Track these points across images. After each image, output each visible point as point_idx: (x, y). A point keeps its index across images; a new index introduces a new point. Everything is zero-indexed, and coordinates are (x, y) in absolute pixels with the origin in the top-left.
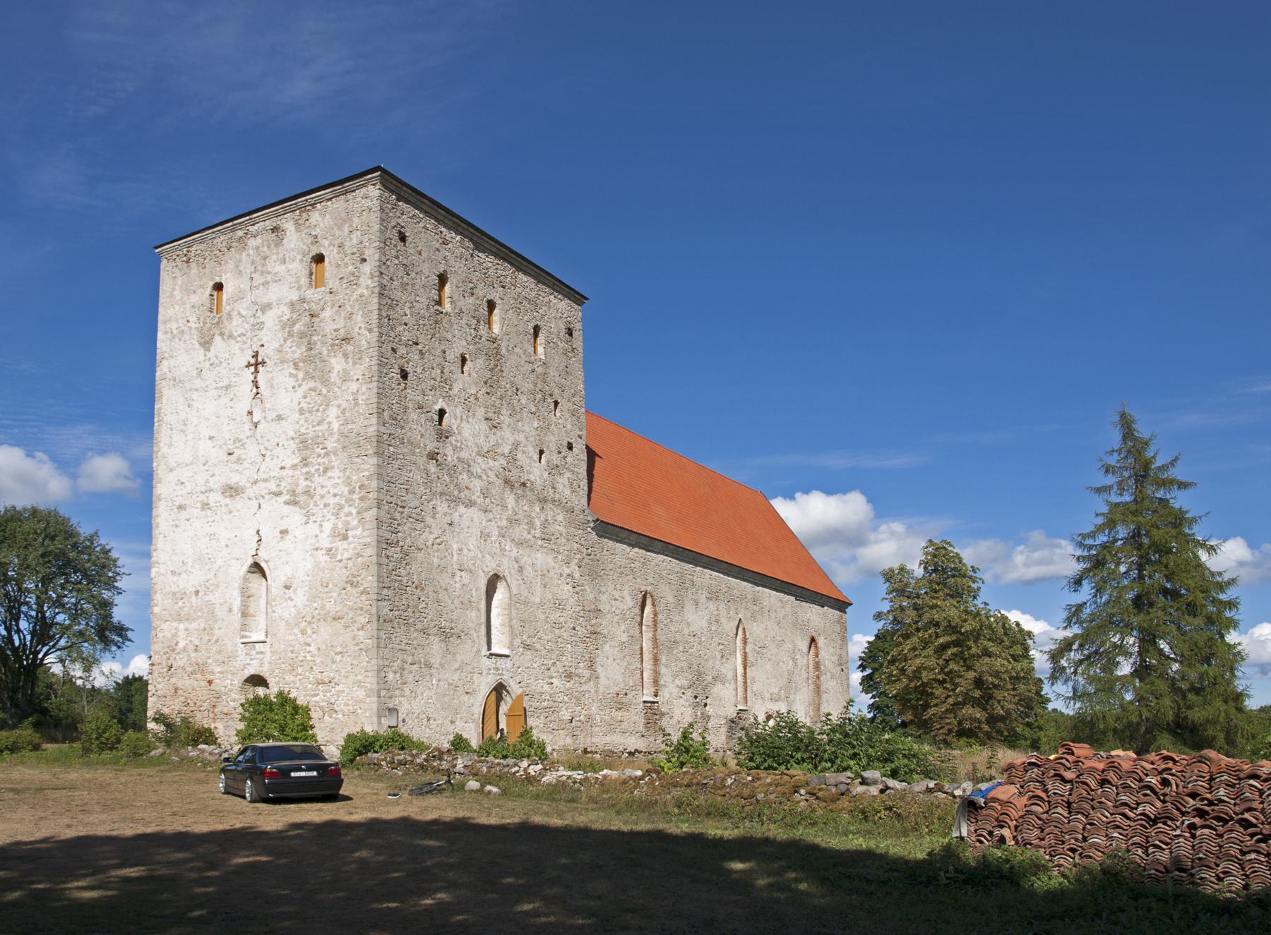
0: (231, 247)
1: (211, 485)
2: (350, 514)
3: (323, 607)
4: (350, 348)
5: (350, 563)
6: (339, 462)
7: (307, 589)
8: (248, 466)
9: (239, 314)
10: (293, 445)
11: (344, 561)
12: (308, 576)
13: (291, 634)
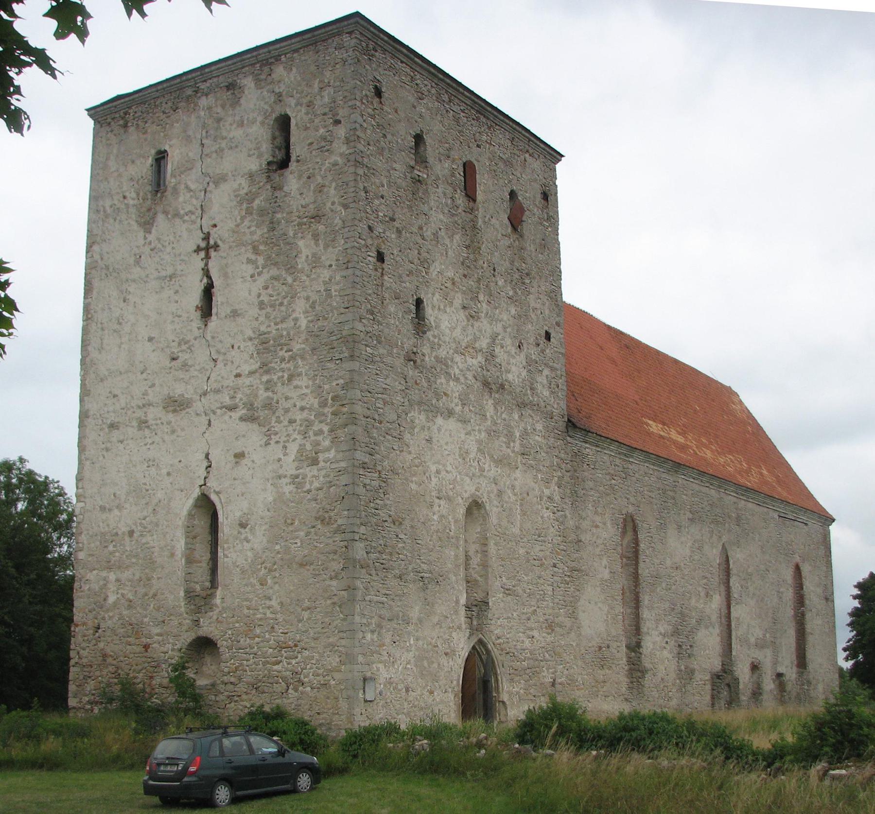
0: (177, 108)
1: (150, 397)
2: (321, 432)
3: (287, 550)
4: (321, 228)
5: (321, 495)
7: (267, 526)
8: (196, 373)
9: (187, 187)
10: (251, 347)
13: (246, 585)
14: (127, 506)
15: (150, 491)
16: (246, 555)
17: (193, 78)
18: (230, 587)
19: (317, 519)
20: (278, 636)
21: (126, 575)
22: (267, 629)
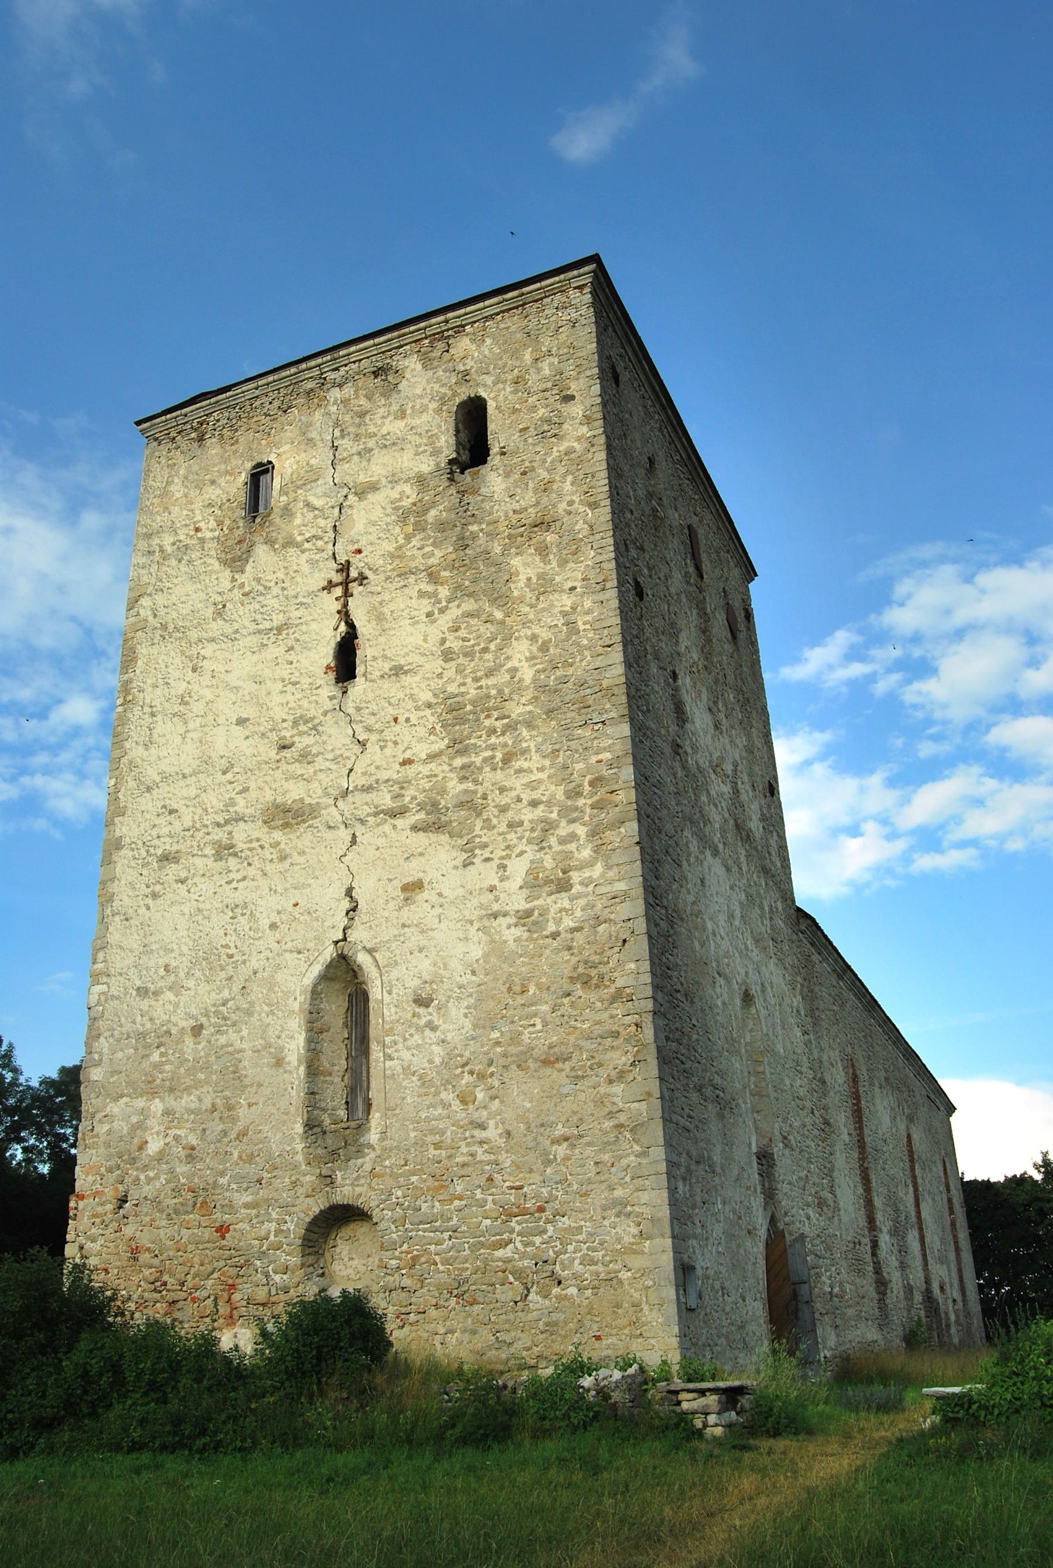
1: (241, 806)
2: (573, 837)
3: (515, 1038)
4: (550, 538)
5: (580, 938)
6: (539, 739)
9: (308, 505)
12: (473, 973)
13: (432, 1106)
14: (191, 983)
18: (397, 1111)
19: (572, 980)
21: (188, 1101)
22: (477, 1183)
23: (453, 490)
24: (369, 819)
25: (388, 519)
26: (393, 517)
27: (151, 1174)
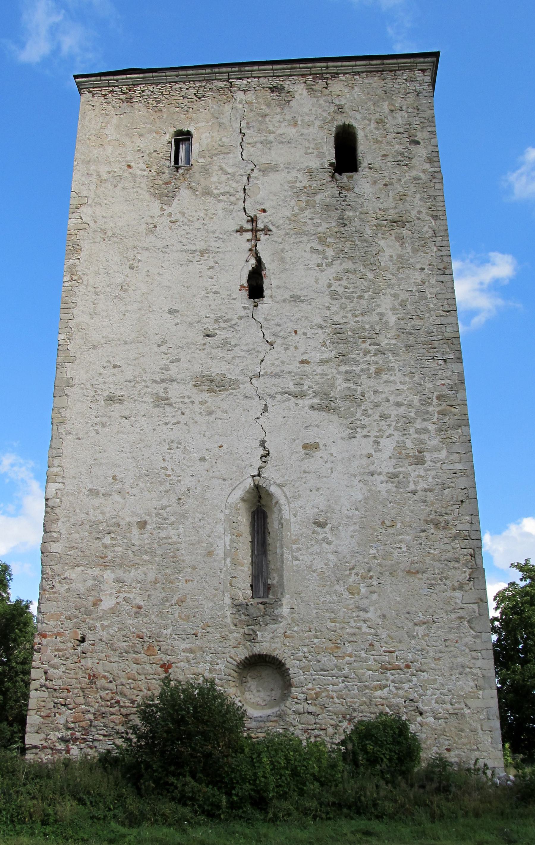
1: (173, 371)
4: (405, 232)
5: (431, 497)
9: (221, 169)
10: (321, 335)
11: (419, 493)
12: (357, 509)
15: (173, 477)
16: (327, 559)
17: (228, 73)
18: (302, 595)
20: (381, 655)
22: (363, 647)
23: (333, 184)
24: (277, 396)
25: (286, 194)
26: (289, 193)
27: (106, 623)
